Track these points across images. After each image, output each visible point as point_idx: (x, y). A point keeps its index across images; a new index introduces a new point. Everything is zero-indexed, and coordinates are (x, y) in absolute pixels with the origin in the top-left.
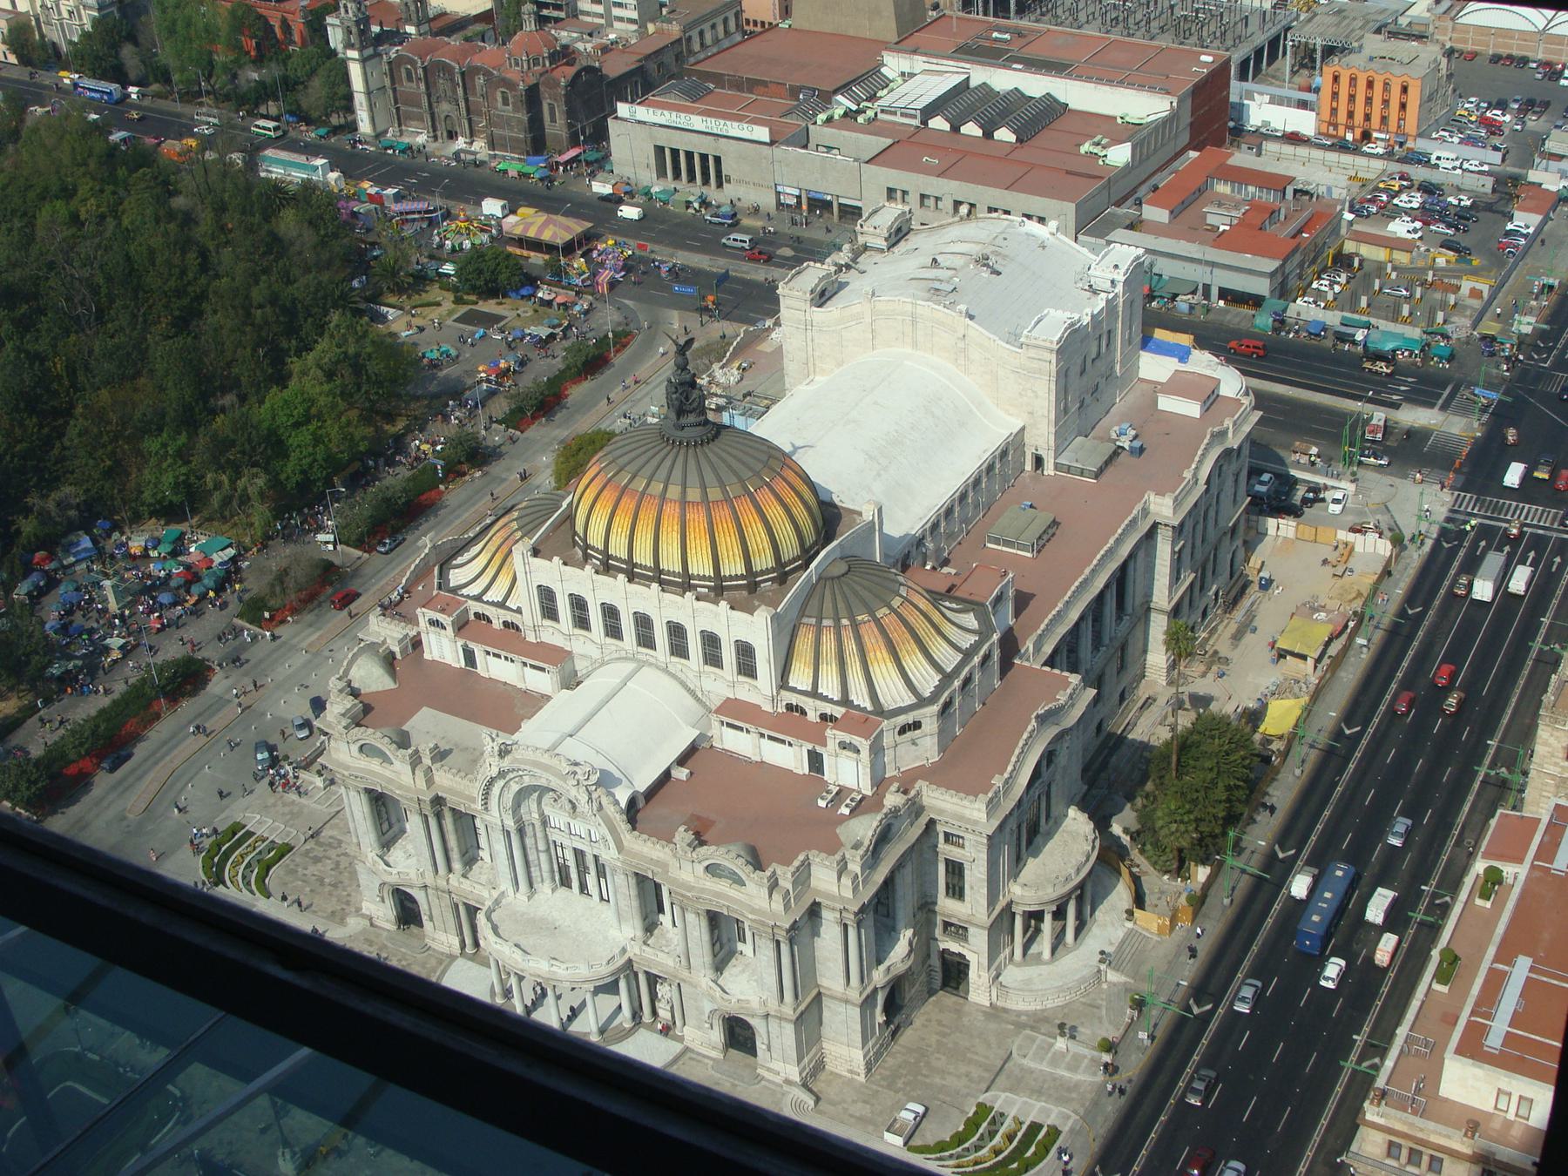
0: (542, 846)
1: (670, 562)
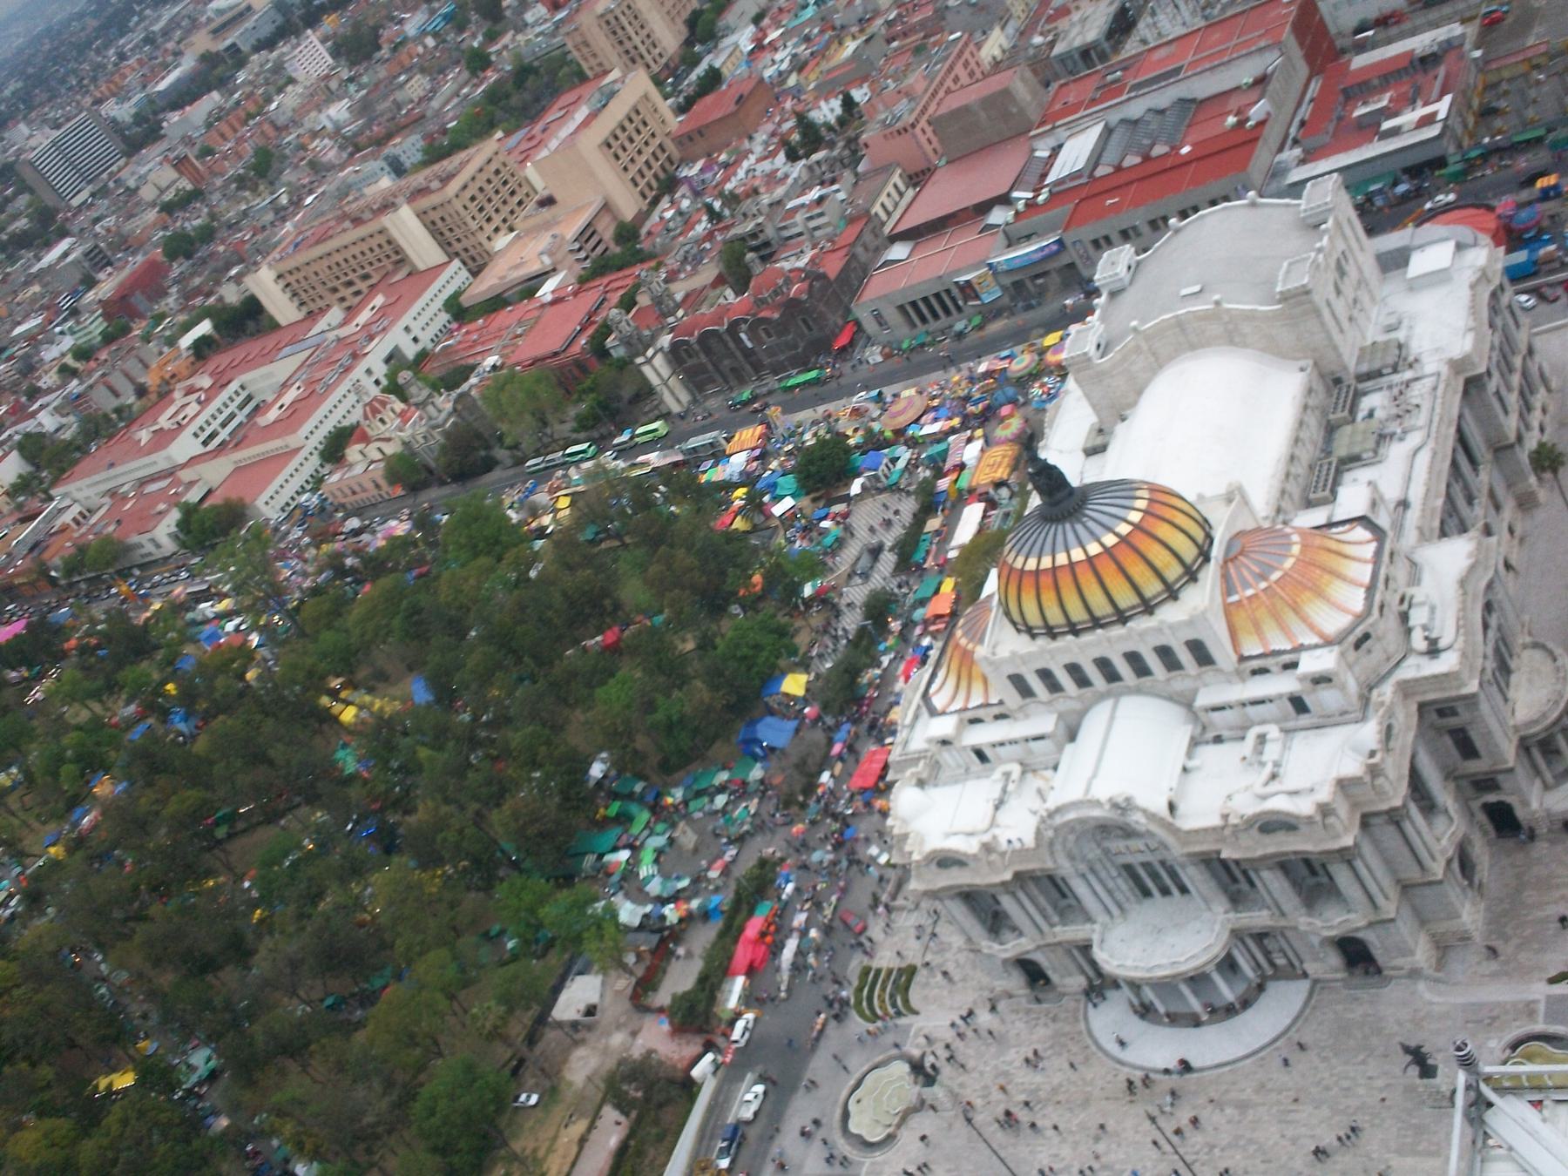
0: (1114, 873)
1: (1101, 606)
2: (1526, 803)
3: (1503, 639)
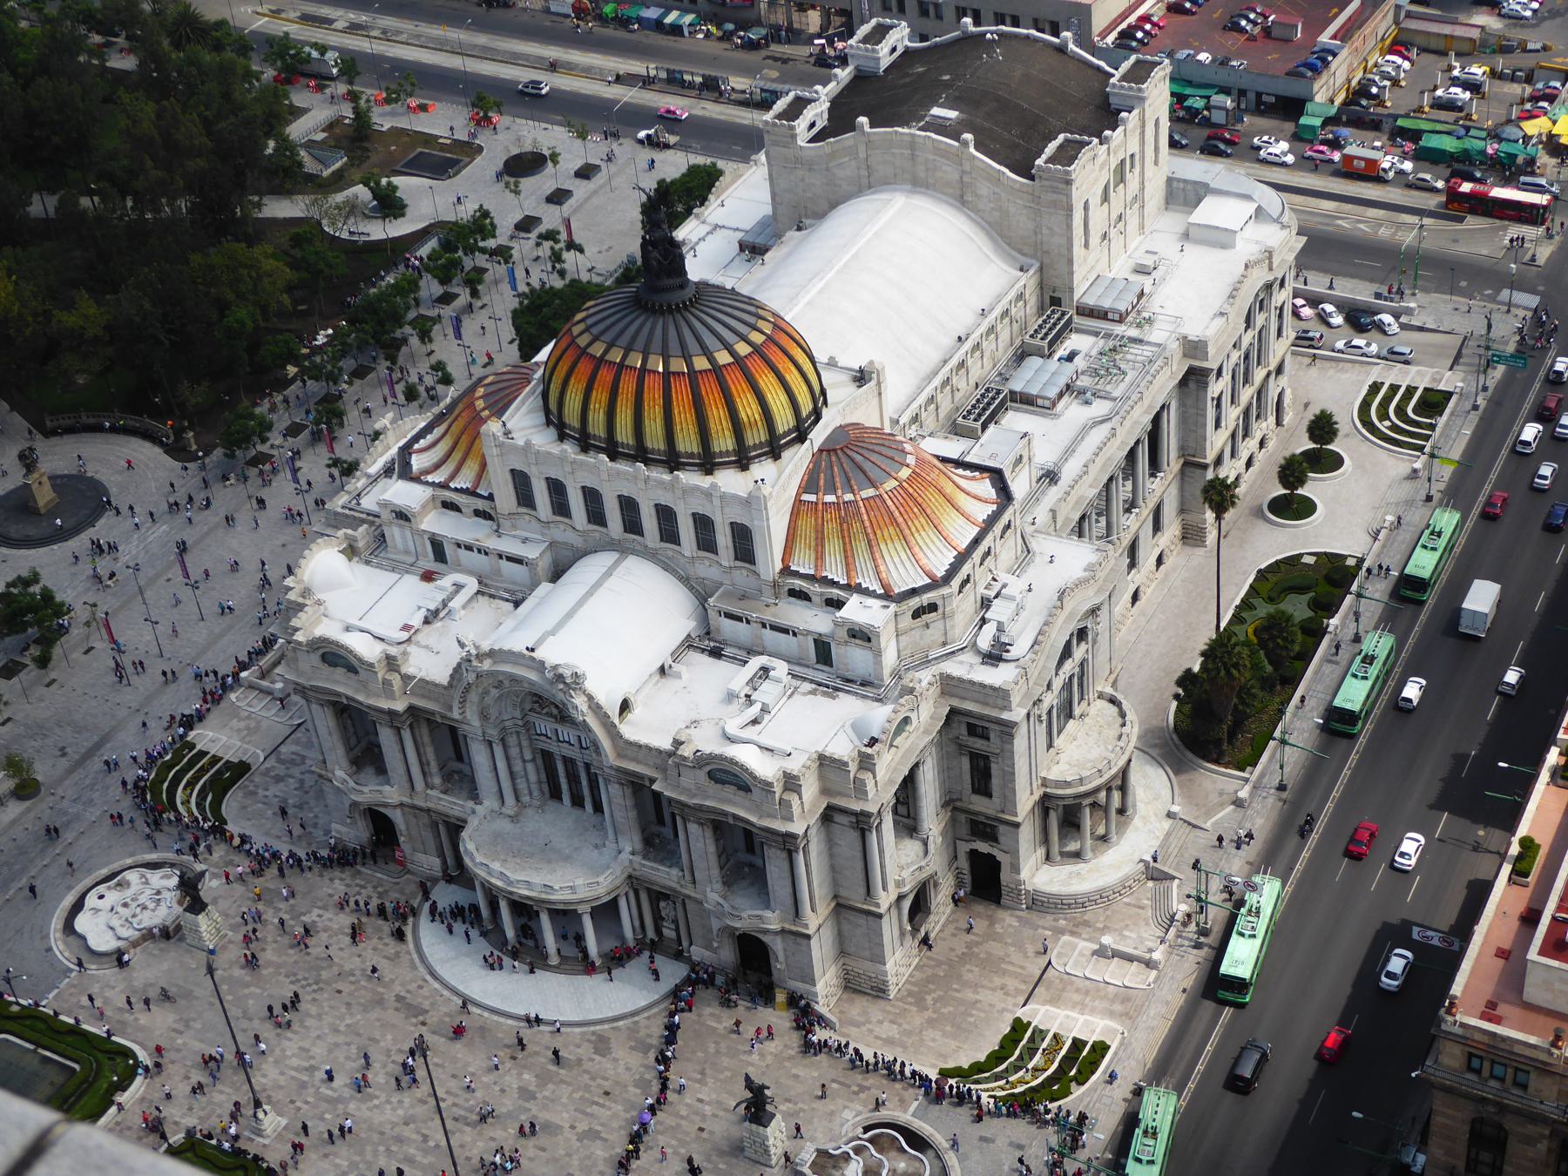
0: (528, 756)
1: (655, 438)
2: (1016, 869)
3: (1081, 678)
